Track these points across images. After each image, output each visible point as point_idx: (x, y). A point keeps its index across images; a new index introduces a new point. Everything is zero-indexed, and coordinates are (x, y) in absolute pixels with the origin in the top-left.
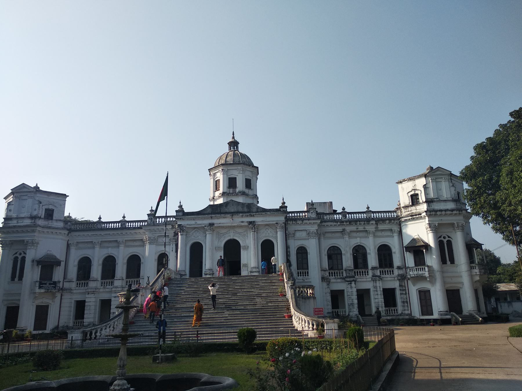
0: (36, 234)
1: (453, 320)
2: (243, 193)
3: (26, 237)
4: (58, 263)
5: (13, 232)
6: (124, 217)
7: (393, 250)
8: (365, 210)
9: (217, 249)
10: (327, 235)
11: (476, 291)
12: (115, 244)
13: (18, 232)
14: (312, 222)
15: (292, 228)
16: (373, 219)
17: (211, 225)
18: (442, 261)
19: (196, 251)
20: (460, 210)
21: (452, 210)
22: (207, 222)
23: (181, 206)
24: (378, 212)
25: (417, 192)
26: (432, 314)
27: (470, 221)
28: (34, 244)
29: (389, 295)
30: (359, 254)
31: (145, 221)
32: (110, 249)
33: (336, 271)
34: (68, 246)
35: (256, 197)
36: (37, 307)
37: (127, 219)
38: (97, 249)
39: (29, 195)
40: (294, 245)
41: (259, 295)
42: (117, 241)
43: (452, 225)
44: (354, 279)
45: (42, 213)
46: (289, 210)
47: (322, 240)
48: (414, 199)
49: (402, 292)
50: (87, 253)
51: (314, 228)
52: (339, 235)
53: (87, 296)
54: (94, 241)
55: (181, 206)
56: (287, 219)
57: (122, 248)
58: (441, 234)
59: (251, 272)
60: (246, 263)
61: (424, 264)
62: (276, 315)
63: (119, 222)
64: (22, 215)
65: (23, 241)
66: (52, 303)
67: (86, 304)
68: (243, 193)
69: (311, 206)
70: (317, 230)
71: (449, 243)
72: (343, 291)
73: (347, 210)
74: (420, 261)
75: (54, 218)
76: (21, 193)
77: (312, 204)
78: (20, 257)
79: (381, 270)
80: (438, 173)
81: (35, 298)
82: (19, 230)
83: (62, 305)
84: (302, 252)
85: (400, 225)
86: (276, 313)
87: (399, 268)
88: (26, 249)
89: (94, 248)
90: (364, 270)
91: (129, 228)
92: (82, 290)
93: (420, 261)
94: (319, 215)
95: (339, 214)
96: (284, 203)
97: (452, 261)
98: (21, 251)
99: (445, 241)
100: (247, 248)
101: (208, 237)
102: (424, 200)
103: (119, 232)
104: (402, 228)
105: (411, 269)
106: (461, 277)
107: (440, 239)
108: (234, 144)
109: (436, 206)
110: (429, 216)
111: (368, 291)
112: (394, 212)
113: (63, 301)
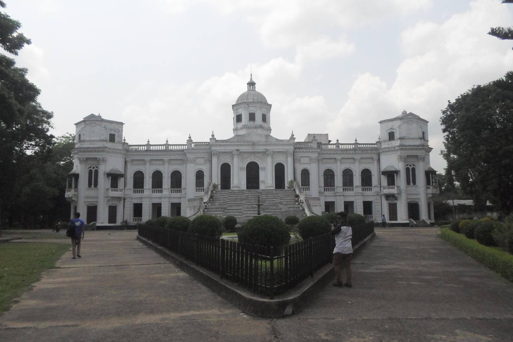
0: (105, 153)
1: (411, 224)
2: (261, 127)
3: (98, 155)
4: (122, 176)
5: (88, 151)
6: (167, 141)
7: (373, 173)
8: (354, 142)
9: (241, 169)
10: (324, 161)
11: (429, 205)
12: (161, 162)
13: (92, 151)
14: (314, 150)
15: (298, 155)
17: (238, 150)
18: (407, 182)
19: (226, 170)
20: (423, 146)
21: (418, 146)
23: (213, 136)
25: (393, 131)
26: (397, 220)
27: (430, 153)
28: (104, 160)
29: (368, 206)
30: (348, 175)
32: (157, 166)
33: (329, 188)
34: (126, 162)
35: (270, 130)
37: (169, 143)
38: (148, 165)
39: (98, 123)
40: (300, 168)
41: (281, 203)
42: (163, 160)
43: (416, 157)
46: (296, 141)
47: (320, 164)
48: (391, 136)
50: (141, 168)
51: (315, 156)
54: (145, 159)
55: (213, 136)
56: (295, 148)
57: (166, 165)
60: (263, 179)
63: (163, 145)
64: (94, 139)
65: (95, 159)
67: (143, 206)
68: (261, 127)
69: (313, 137)
70: (317, 157)
71: (414, 169)
72: (333, 203)
73: (340, 142)
74: (391, 182)
75: (116, 141)
76: (92, 121)
77: (314, 136)
78: (93, 170)
80: (410, 117)
81: (108, 201)
83: (126, 206)
84: (305, 173)
85: (379, 154)
87: (376, 186)
89: (145, 164)
90: (350, 188)
91: (172, 151)
92: (139, 195)
93: (391, 182)
94: (319, 144)
96: (293, 135)
97: (414, 183)
99: (411, 168)
100: (264, 169)
101: (236, 159)
103: (165, 153)
108: (251, 84)
109: (407, 143)
110: (401, 149)
111: (352, 203)
112: (375, 144)
113: (126, 203)
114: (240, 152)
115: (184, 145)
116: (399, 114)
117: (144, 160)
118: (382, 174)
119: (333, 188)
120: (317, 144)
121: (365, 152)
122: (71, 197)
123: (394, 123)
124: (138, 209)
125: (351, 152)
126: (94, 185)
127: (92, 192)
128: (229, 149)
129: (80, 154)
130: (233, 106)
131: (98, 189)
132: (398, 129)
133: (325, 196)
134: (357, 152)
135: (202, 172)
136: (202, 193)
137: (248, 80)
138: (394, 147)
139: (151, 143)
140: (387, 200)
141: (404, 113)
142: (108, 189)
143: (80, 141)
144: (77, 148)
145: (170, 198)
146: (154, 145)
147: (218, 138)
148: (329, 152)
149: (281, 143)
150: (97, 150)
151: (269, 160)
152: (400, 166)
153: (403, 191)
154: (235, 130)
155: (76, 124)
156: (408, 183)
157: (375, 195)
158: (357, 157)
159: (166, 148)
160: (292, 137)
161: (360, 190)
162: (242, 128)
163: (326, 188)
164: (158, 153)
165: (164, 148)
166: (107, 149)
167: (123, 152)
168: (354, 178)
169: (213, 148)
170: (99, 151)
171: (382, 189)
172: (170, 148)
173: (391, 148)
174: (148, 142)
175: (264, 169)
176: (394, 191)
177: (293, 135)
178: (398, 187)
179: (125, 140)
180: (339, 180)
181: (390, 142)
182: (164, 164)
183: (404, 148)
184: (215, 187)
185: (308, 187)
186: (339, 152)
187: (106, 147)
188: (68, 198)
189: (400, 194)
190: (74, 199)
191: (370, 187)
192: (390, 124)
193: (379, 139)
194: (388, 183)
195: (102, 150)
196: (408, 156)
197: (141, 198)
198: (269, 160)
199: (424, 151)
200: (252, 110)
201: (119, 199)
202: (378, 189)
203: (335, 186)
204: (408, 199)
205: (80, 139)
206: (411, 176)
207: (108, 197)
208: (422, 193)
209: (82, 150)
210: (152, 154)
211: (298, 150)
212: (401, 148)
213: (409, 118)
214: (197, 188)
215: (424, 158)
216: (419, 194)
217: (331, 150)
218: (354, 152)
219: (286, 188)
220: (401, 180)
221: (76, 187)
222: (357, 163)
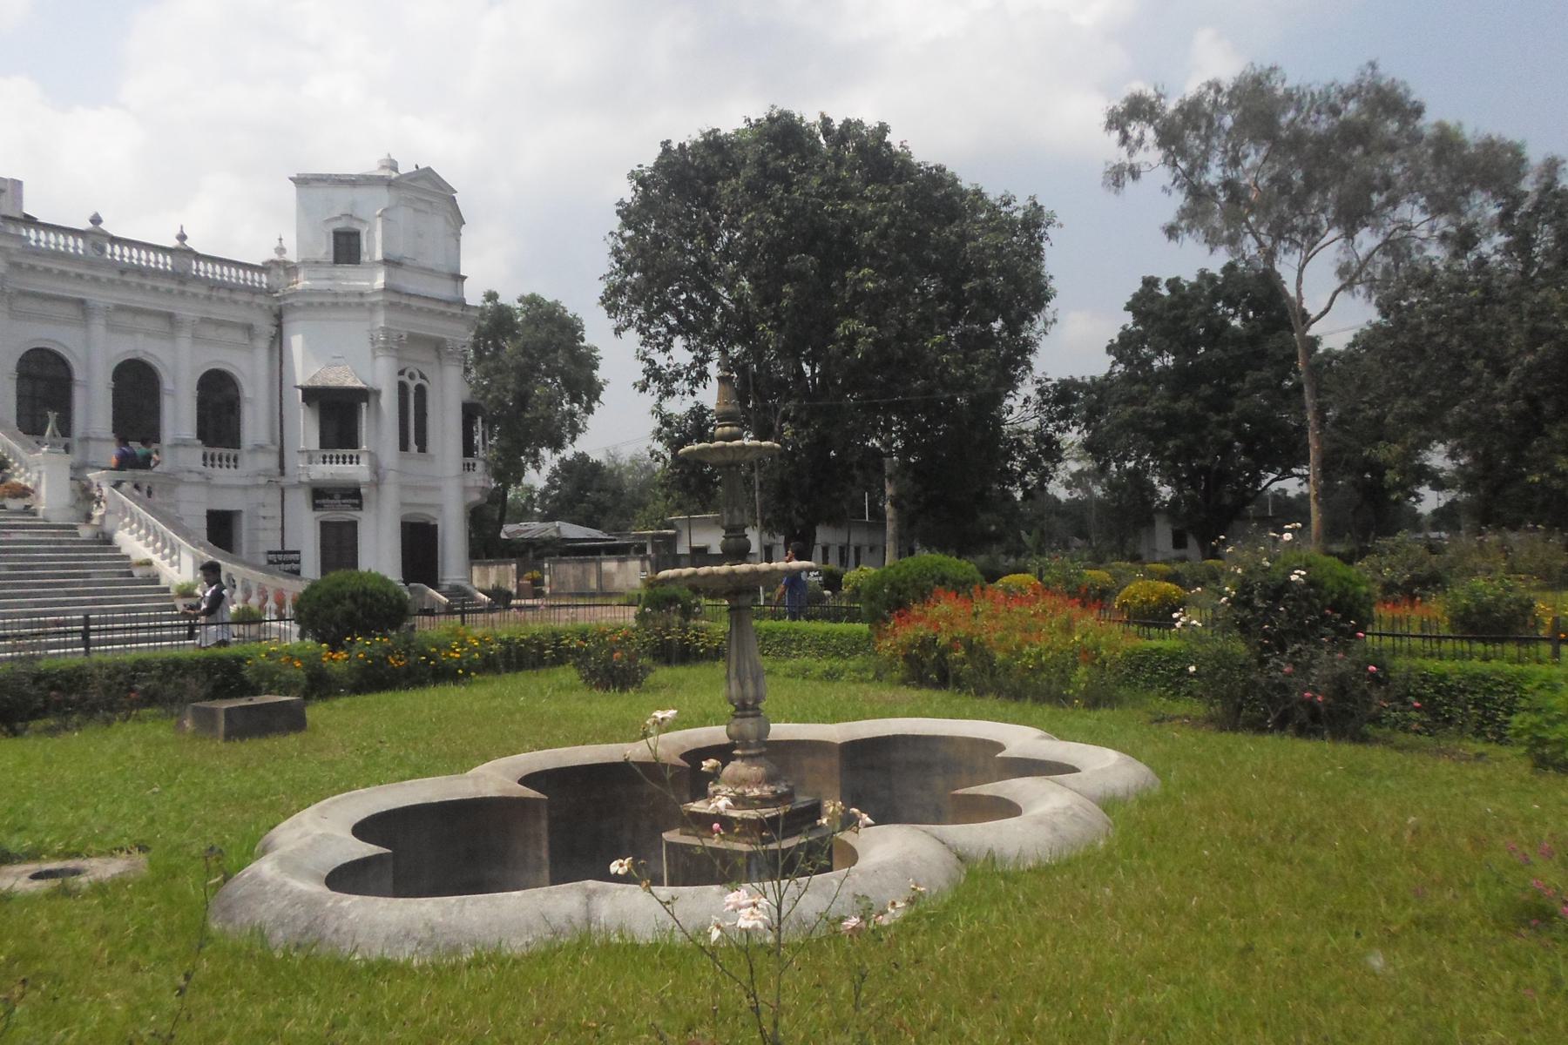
7: (247, 392)
8: (172, 243)
16: (197, 278)
21: (448, 303)
25: (356, 226)
30: (137, 389)
48: (347, 247)
49: (262, 523)
52: (70, 311)
58: (406, 364)
61: (354, 444)
62: (87, 575)
71: (421, 390)
73: (109, 227)
85: (279, 318)
86: (82, 567)
87: (259, 448)
97: (422, 447)
99: (412, 385)
102: (379, 256)
104: (287, 328)
106: (438, 489)
107: (402, 378)
110: (392, 306)
121: (224, 294)
123: (360, 194)
125: (164, 285)
132: (379, 223)
134: (190, 289)
138: (361, 294)
140: (316, 507)
148: (57, 266)
152: (379, 374)
153: (391, 477)
156: (404, 446)
157: (258, 486)
158: (187, 311)
161: (193, 457)
168: (167, 406)
173: (346, 295)
176: (356, 471)
178: (372, 455)
183: (404, 301)
186: (103, 275)
189: (377, 480)
191: (232, 452)
192: (344, 196)
193: (281, 250)
194: (322, 438)
196: (414, 339)
202: (269, 462)
204: (403, 504)
212: (395, 298)
217: (57, 255)
218: (174, 286)
220: (379, 430)
222: (184, 342)
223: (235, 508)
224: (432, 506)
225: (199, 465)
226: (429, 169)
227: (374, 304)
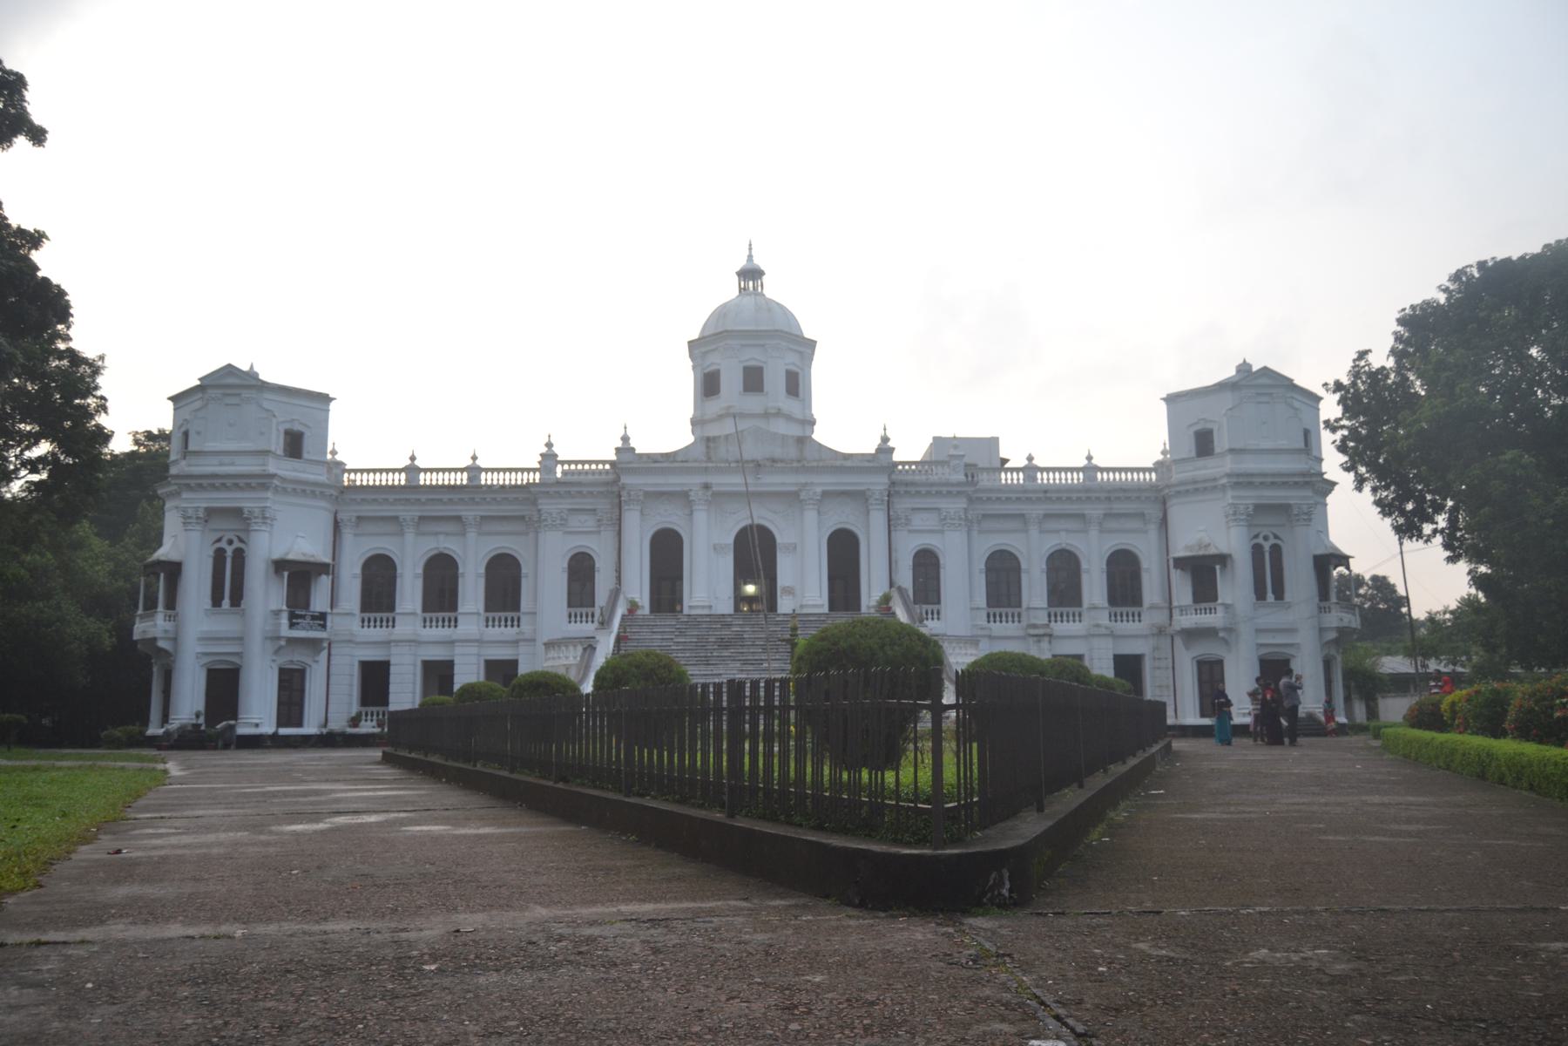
0: (269, 494)
3: (246, 501)
4: (323, 568)
6: (474, 458)
7: (1144, 565)
8: (1082, 463)
9: (717, 548)
11: (1328, 664)
14: (955, 489)
15: (902, 505)
17: (707, 486)
19: (667, 554)
22: (693, 481)
23: (625, 439)
24: (1114, 470)
25: (1209, 426)
27: (1330, 499)
31: (534, 470)
32: (441, 537)
33: (1003, 610)
34: (337, 526)
36: (282, 671)
37: (481, 463)
38: (410, 537)
39: (246, 394)
42: (458, 519)
43: (1284, 509)
44: (1048, 631)
45: (277, 444)
46: (896, 457)
47: (975, 533)
48: (1204, 443)
53: (394, 650)
55: (625, 439)
56: (893, 484)
57: (472, 535)
59: (802, 606)
63: (462, 470)
65: (237, 513)
66: (314, 666)
67: (392, 669)
71: (1276, 551)
73: (1038, 462)
74: (1205, 592)
75: (305, 455)
76: (228, 389)
77: (955, 442)
78: (229, 550)
79: (1114, 609)
81: (276, 652)
82: (229, 482)
84: (927, 564)
85: (1164, 503)
87: (1152, 607)
88: (247, 531)
89: (401, 534)
90: (1071, 610)
91: (490, 488)
93: (1205, 592)
94: (971, 470)
95: (1018, 470)
96: (885, 439)
97: (1279, 593)
98: (231, 535)
99: (1267, 546)
101: (701, 516)
102: (1227, 447)
103: (465, 496)
105: (1183, 610)
108: (751, 274)
110: (1237, 485)
112: (1149, 470)
114: (717, 495)
115: (529, 470)
116: (1229, 372)
117: (396, 518)
118: (1176, 567)
119: (1016, 610)
120: (964, 471)
122: (155, 639)
124: (375, 679)
126: (232, 598)
127: (225, 624)
128: (675, 482)
129: (184, 495)
130: (691, 343)
131: (243, 614)
133: (990, 637)
135: (590, 558)
136: (587, 628)
137: (741, 263)
138: (1215, 479)
139: (420, 463)
141: (1244, 368)
142: (277, 613)
143: (186, 452)
144: (177, 477)
145: (480, 642)
146: (431, 470)
147: (642, 446)
149: (848, 463)
150: (241, 482)
151: (811, 516)
152: (1231, 540)
154: (696, 423)
155: (174, 399)
156: (1260, 594)
159: (469, 479)
160: (885, 449)
162: (720, 417)
163: (992, 611)
164: (446, 497)
165: (463, 479)
166: (276, 482)
167: (328, 492)
168: (1085, 578)
169: (625, 480)
170: (249, 487)
171: (1176, 613)
172: (486, 479)
173: (1205, 481)
174: (413, 458)
175: (792, 548)
176: (1212, 619)
177: (885, 439)
178: (1227, 607)
179: (334, 453)
180: (1035, 590)
181: (1202, 462)
182: (464, 535)
184: (633, 607)
185: (935, 607)
187: (273, 476)
188: (143, 641)
190: (161, 644)
191: (1136, 610)
193: (1164, 453)
195: (262, 482)
196: (1259, 508)
197: (387, 643)
198: (811, 516)
199: (1309, 493)
200: (753, 357)
201: (314, 645)
203: (1024, 605)
205: (186, 446)
206: (1269, 577)
207: (279, 638)
208: (1301, 630)
209: (192, 482)
210: (423, 498)
211: (902, 489)
213: (1260, 387)
214: (573, 611)
215: (1309, 513)
216: (1292, 631)
217: (1010, 488)
219: (864, 609)
220: (1235, 589)
221: (171, 604)
222: (1094, 532)
223: (1137, 652)
224: (1291, 645)
225: (1104, 621)
226: (1265, 368)
227: (1224, 486)
